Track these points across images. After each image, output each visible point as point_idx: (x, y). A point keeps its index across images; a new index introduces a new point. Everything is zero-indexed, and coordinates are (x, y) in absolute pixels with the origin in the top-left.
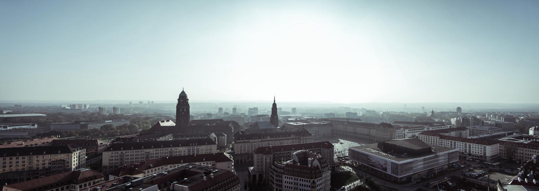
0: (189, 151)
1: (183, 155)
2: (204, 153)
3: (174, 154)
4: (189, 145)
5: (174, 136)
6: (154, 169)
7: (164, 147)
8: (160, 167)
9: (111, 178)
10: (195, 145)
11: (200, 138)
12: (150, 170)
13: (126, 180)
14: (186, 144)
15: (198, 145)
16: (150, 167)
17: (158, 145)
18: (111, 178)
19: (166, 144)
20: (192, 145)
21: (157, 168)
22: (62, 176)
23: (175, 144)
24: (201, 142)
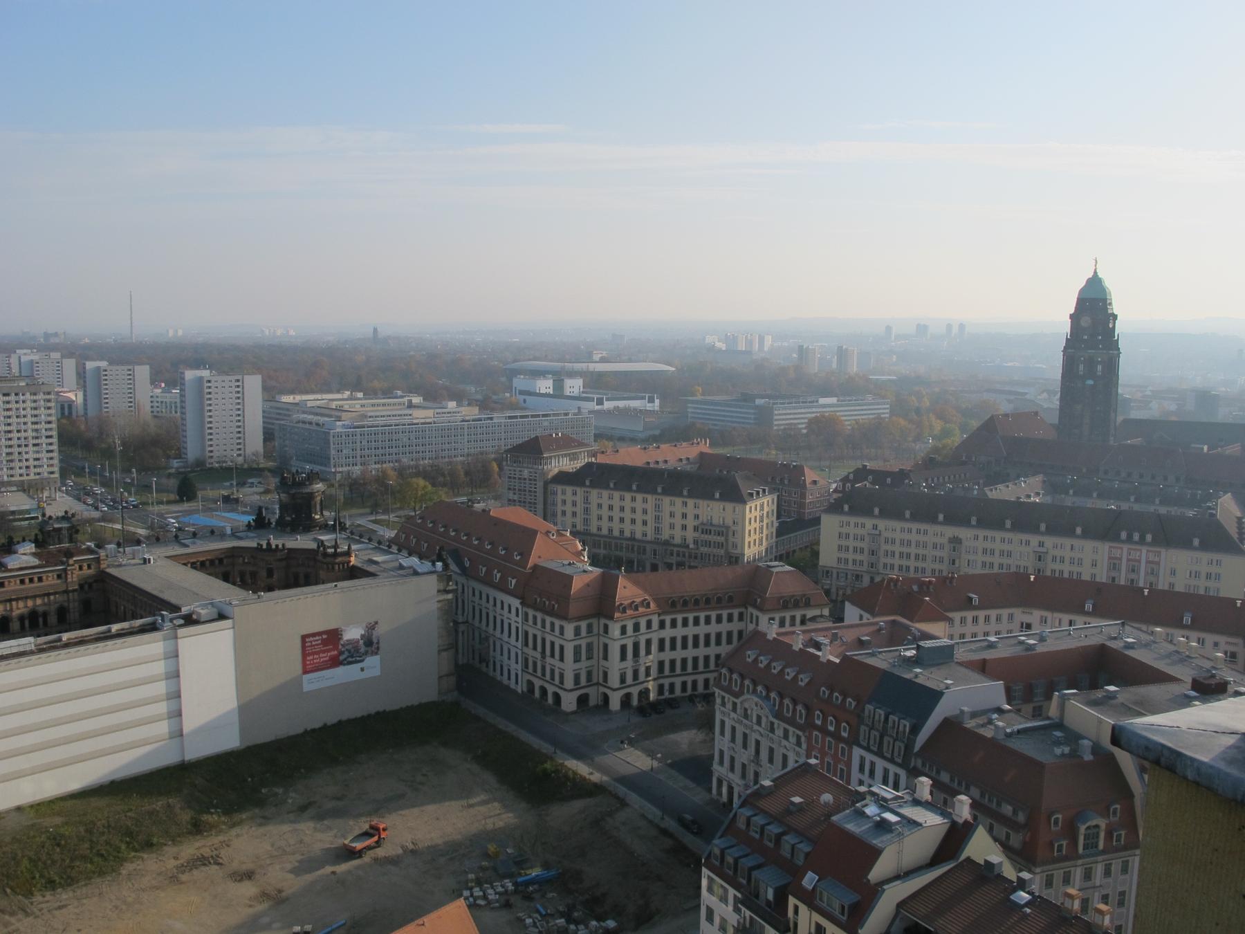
0: (1114, 566)
1: (1086, 577)
2: (1179, 588)
3: (1050, 567)
4: (1116, 538)
5: (1053, 487)
6: (981, 614)
7: (1017, 527)
8: (1005, 612)
9: (852, 613)
10: (1142, 541)
11: (1163, 510)
12: (969, 615)
13: (896, 636)
14: (1106, 529)
15: (1155, 542)
16: (968, 604)
17: (994, 517)
18: (852, 613)
19: (1022, 518)
20: (1130, 539)
21: (993, 613)
22: (724, 576)
23: (1059, 523)
24: (1169, 534)
